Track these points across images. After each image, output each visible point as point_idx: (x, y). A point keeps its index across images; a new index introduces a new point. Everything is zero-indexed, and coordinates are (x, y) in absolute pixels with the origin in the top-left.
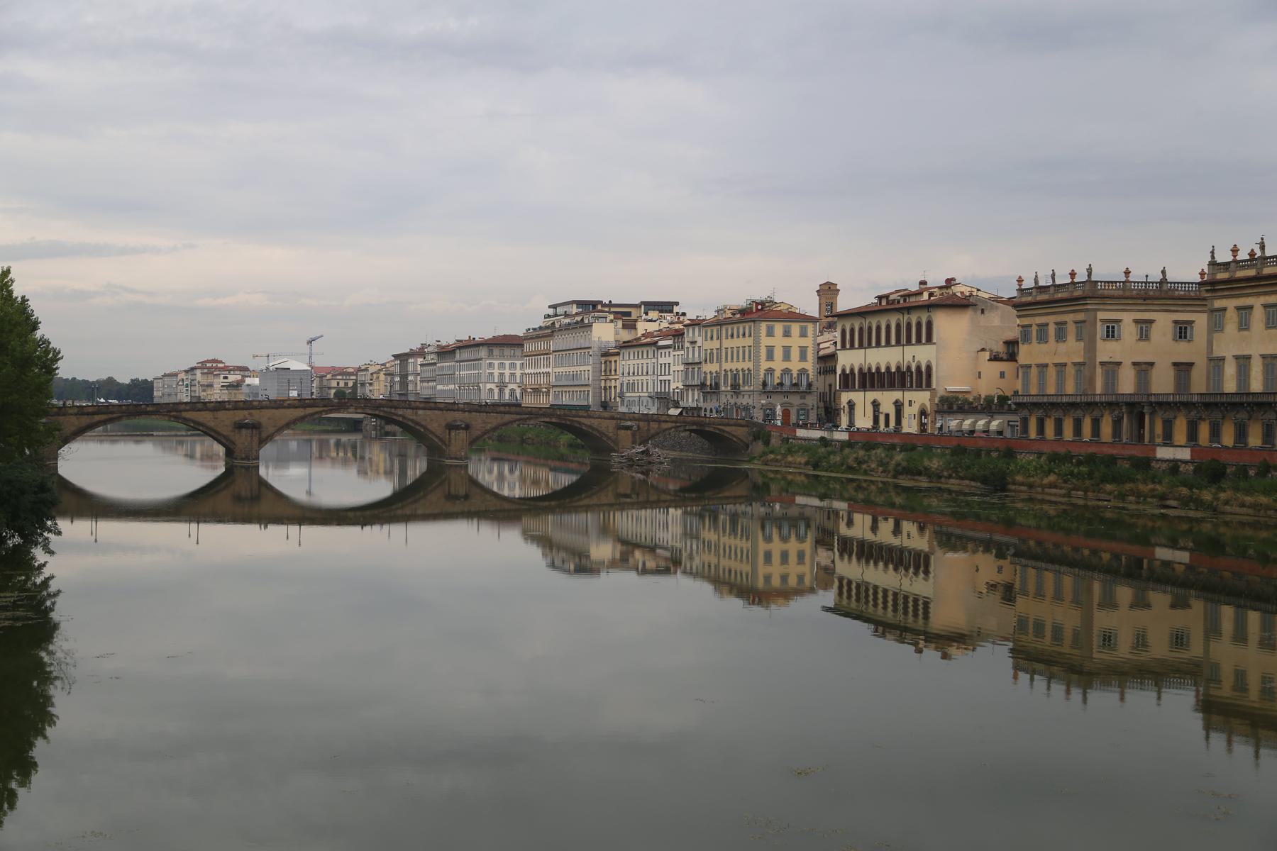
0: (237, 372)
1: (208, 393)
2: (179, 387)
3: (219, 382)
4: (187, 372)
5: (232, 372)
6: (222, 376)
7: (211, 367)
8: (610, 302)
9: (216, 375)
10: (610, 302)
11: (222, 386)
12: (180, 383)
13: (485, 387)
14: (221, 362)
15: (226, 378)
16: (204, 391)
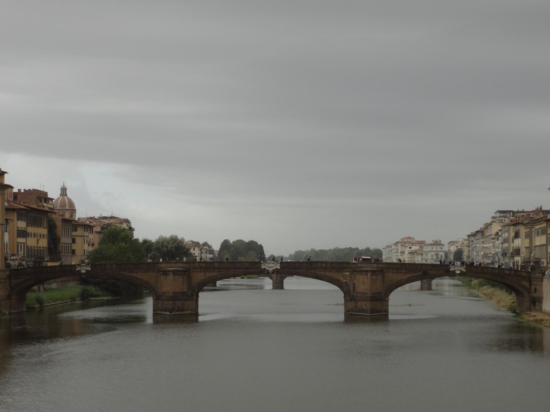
0: (418, 245)
1: (403, 257)
2: (392, 253)
3: (407, 250)
4: (395, 244)
5: (414, 245)
6: (408, 247)
7: (406, 242)
8: (523, 210)
9: (406, 246)
10: (523, 210)
11: (409, 253)
12: (392, 251)
13: (480, 254)
14: (413, 238)
15: (410, 248)
16: (401, 255)
